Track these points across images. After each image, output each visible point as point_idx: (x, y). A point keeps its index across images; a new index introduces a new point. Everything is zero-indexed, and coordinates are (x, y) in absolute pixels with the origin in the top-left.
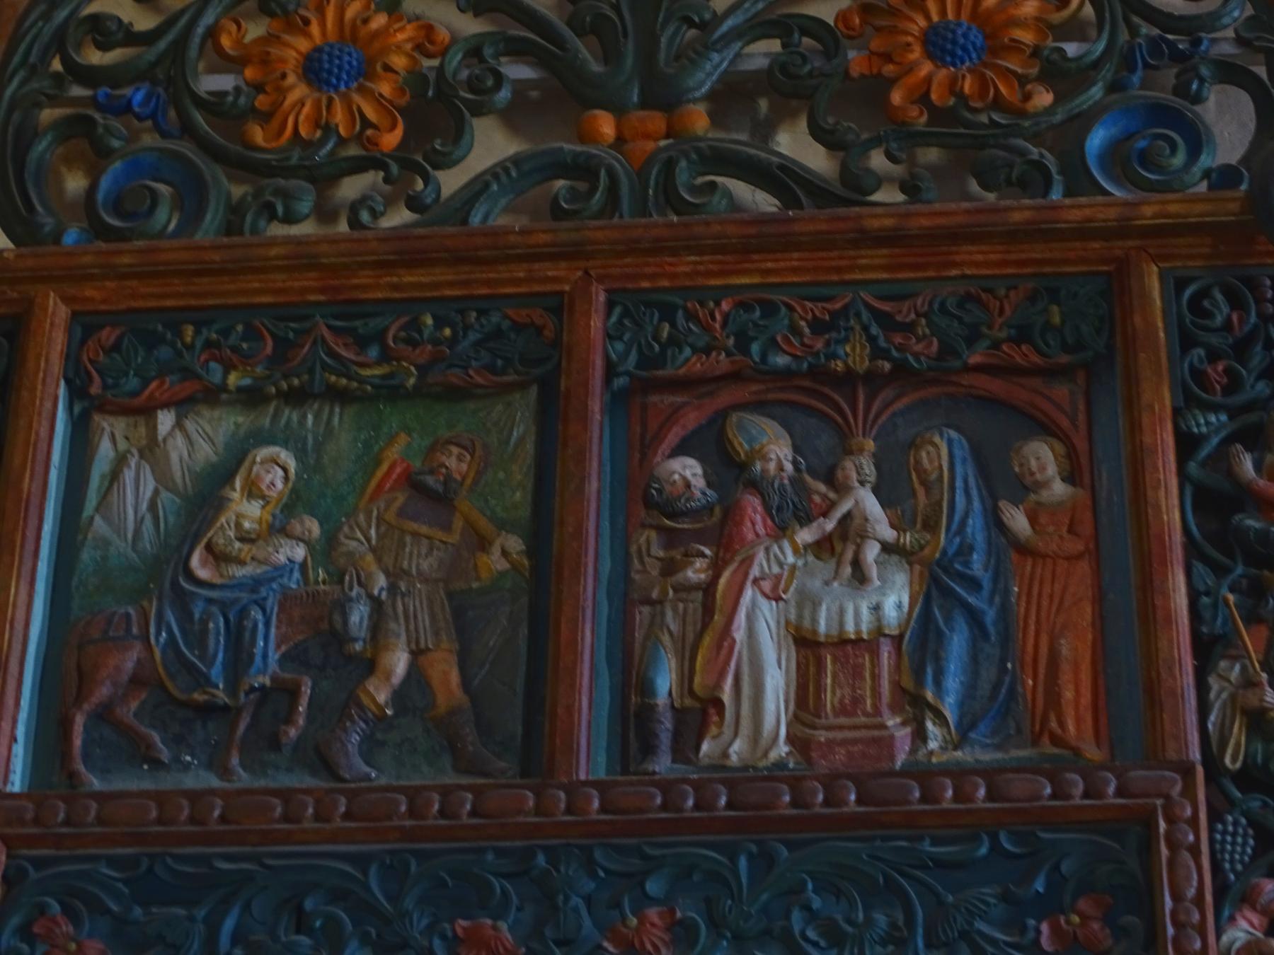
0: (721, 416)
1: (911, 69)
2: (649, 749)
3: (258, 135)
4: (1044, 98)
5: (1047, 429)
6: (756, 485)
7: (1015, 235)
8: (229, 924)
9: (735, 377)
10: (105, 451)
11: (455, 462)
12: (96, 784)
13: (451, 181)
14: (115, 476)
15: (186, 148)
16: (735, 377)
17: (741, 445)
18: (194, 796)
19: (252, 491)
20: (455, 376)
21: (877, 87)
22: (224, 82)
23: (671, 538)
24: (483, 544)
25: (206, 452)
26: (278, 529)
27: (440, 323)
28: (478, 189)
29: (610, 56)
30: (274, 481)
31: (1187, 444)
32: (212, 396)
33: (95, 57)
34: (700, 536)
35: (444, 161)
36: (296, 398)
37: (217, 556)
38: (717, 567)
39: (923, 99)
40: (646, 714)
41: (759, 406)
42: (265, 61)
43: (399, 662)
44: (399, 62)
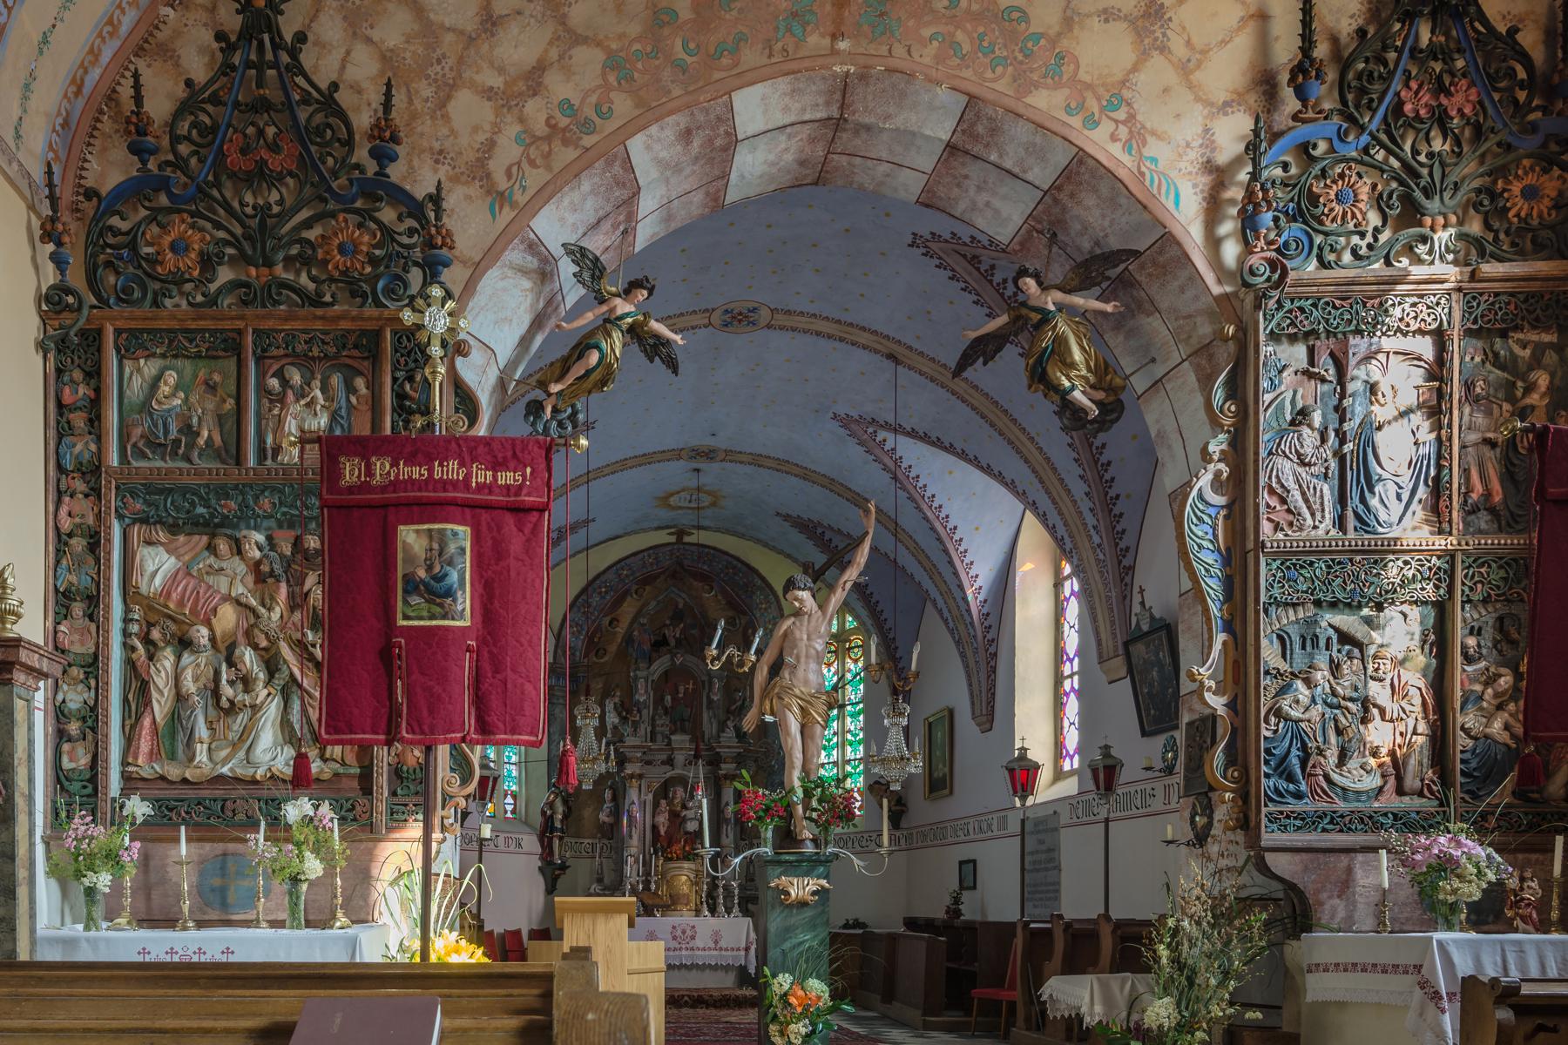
0: (283, 366)
1: (334, 257)
2: (265, 458)
3: (159, 269)
4: (368, 269)
5: (361, 374)
6: (291, 387)
7: (353, 319)
8: (169, 501)
9: (286, 356)
10: (127, 371)
11: (217, 377)
12: (135, 464)
13: (213, 287)
14: (131, 378)
15: (139, 272)
16: (286, 356)
17: (287, 376)
18: (158, 469)
19: (166, 384)
20: (215, 353)
21: (325, 262)
22: (149, 250)
23: (271, 401)
24: (224, 401)
25: (154, 372)
26: (173, 395)
27: (211, 336)
28: (219, 291)
29: (254, 249)
30: (172, 381)
31: (395, 380)
32: (153, 355)
33: (110, 240)
34: (278, 401)
35: (211, 281)
36: (175, 356)
37: (159, 403)
38: (282, 410)
39: (337, 267)
40: (264, 450)
41: (292, 364)
42: (159, 244)
43: (205, 434)
44: (196, 247)
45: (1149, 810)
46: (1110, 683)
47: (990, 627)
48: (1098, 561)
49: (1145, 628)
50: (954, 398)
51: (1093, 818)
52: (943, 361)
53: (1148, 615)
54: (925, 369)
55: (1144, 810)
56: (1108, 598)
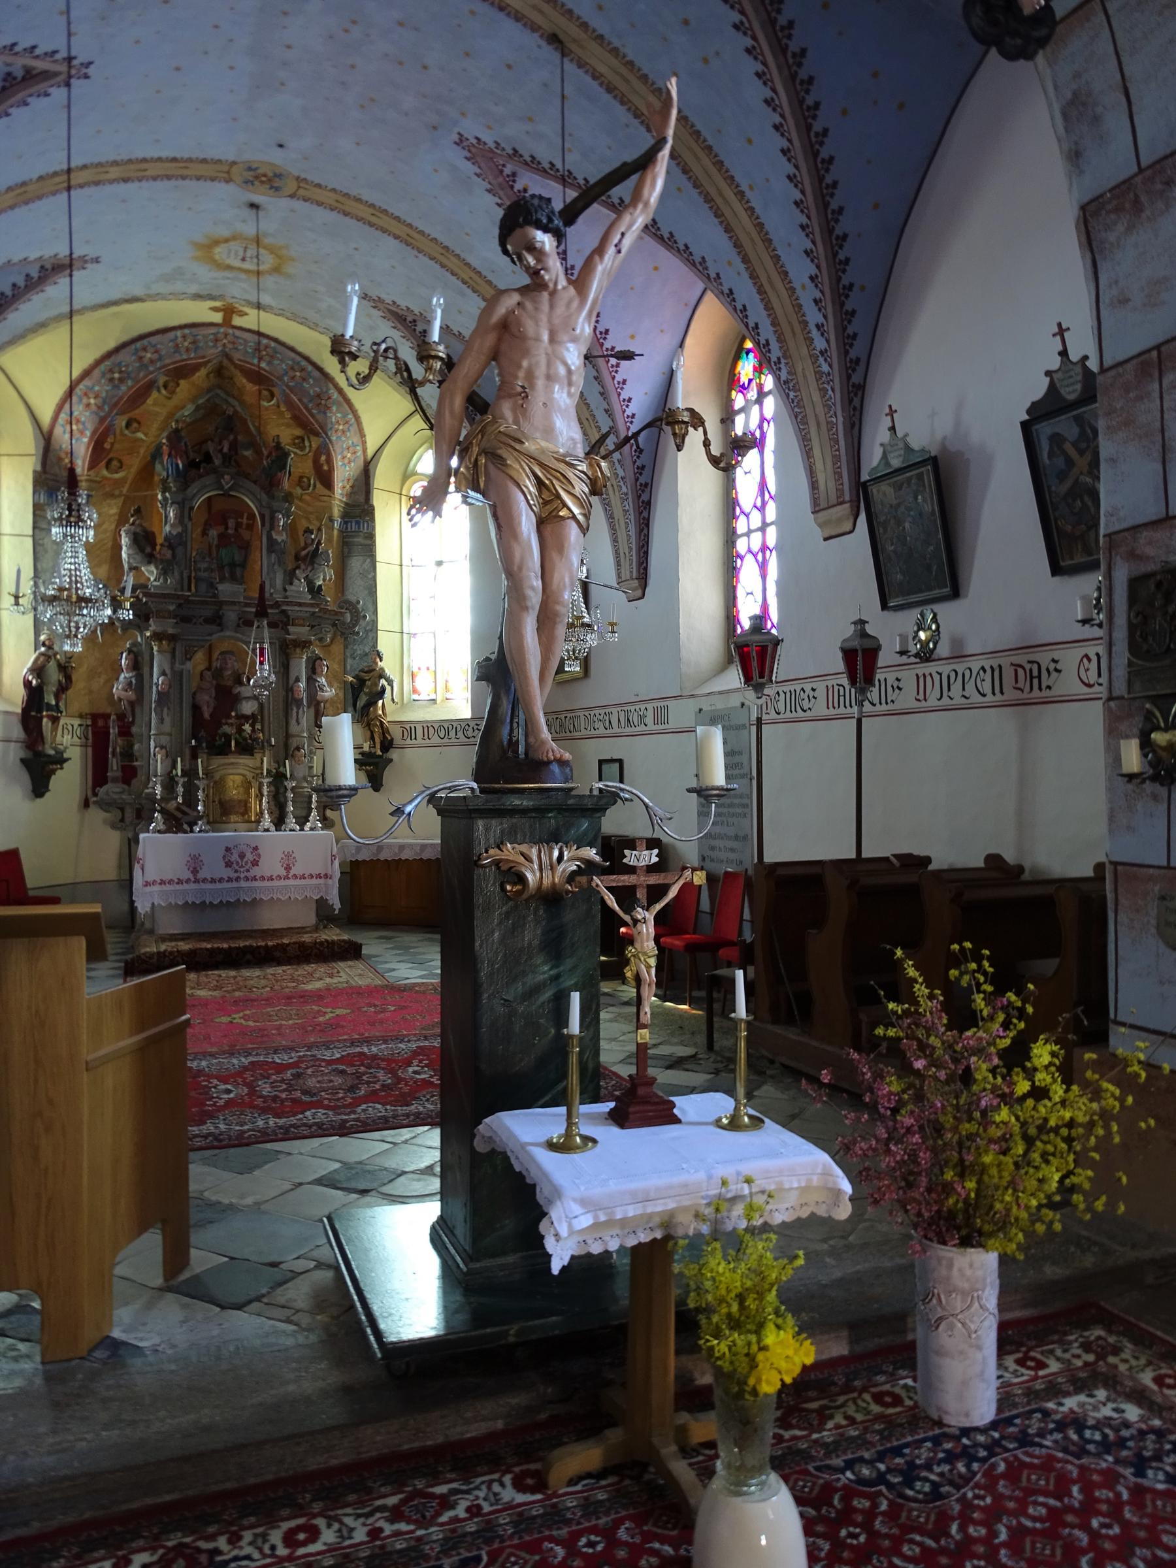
45: (891, 706)
46: (826, 539)
47: (643, 467)
48: (819, 374)
49: (896, 463)
50: (636, 122)
51: (800, 714)
52: (630, 57)
53: (901, 445)
54: (602, 69)
55: (884, 707)
56: (831, 426)
